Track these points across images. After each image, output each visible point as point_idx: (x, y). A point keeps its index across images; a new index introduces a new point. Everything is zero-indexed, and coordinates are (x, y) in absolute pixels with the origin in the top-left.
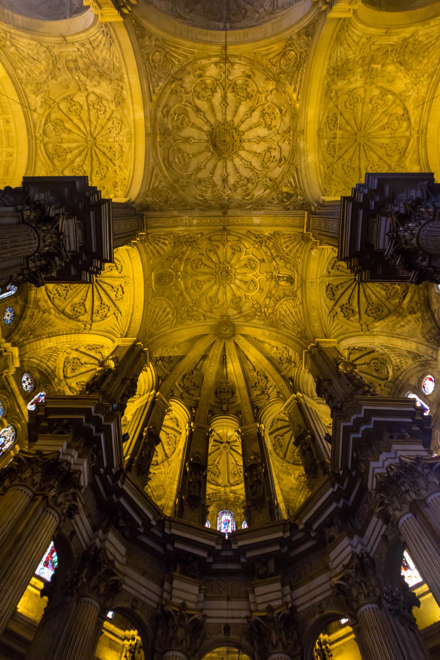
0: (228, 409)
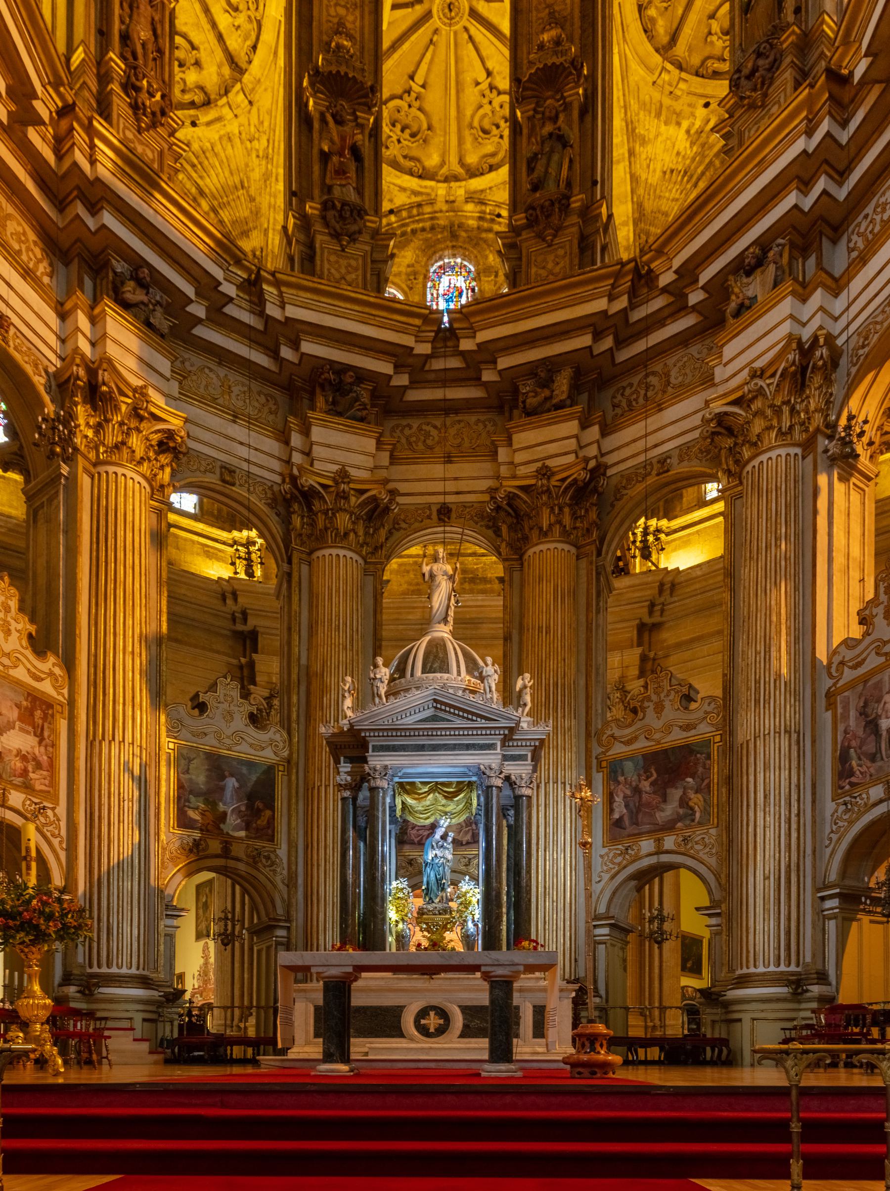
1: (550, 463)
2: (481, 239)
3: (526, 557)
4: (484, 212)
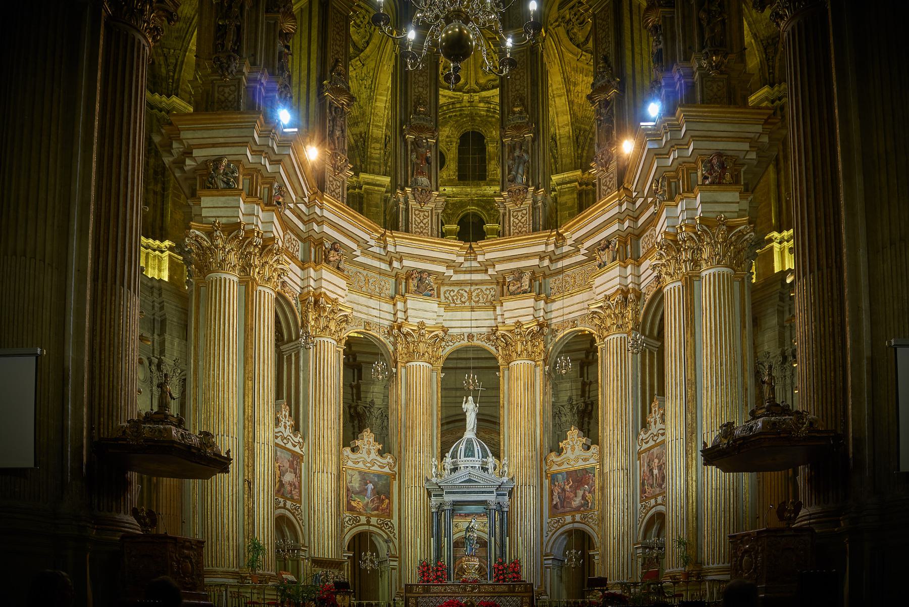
1: (520, 319)
2: (488, 121)
3: (510, 365)
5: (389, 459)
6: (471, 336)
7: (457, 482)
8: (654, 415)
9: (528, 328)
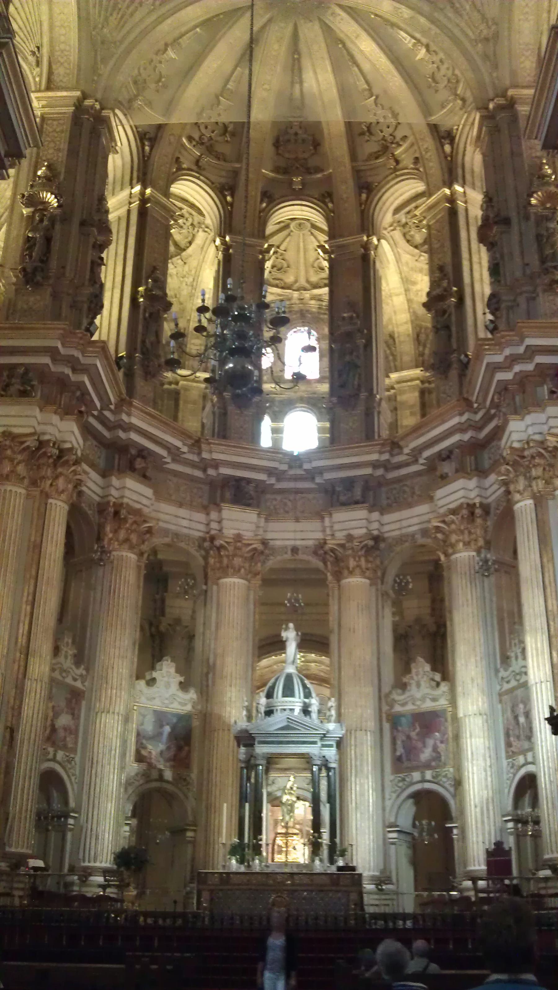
0: (303, 183)
4: (322, 305)
5: (192, 695)
6: (295, 550)
7: (272, 729)
8: (514, 649)
9: (360, 542)
